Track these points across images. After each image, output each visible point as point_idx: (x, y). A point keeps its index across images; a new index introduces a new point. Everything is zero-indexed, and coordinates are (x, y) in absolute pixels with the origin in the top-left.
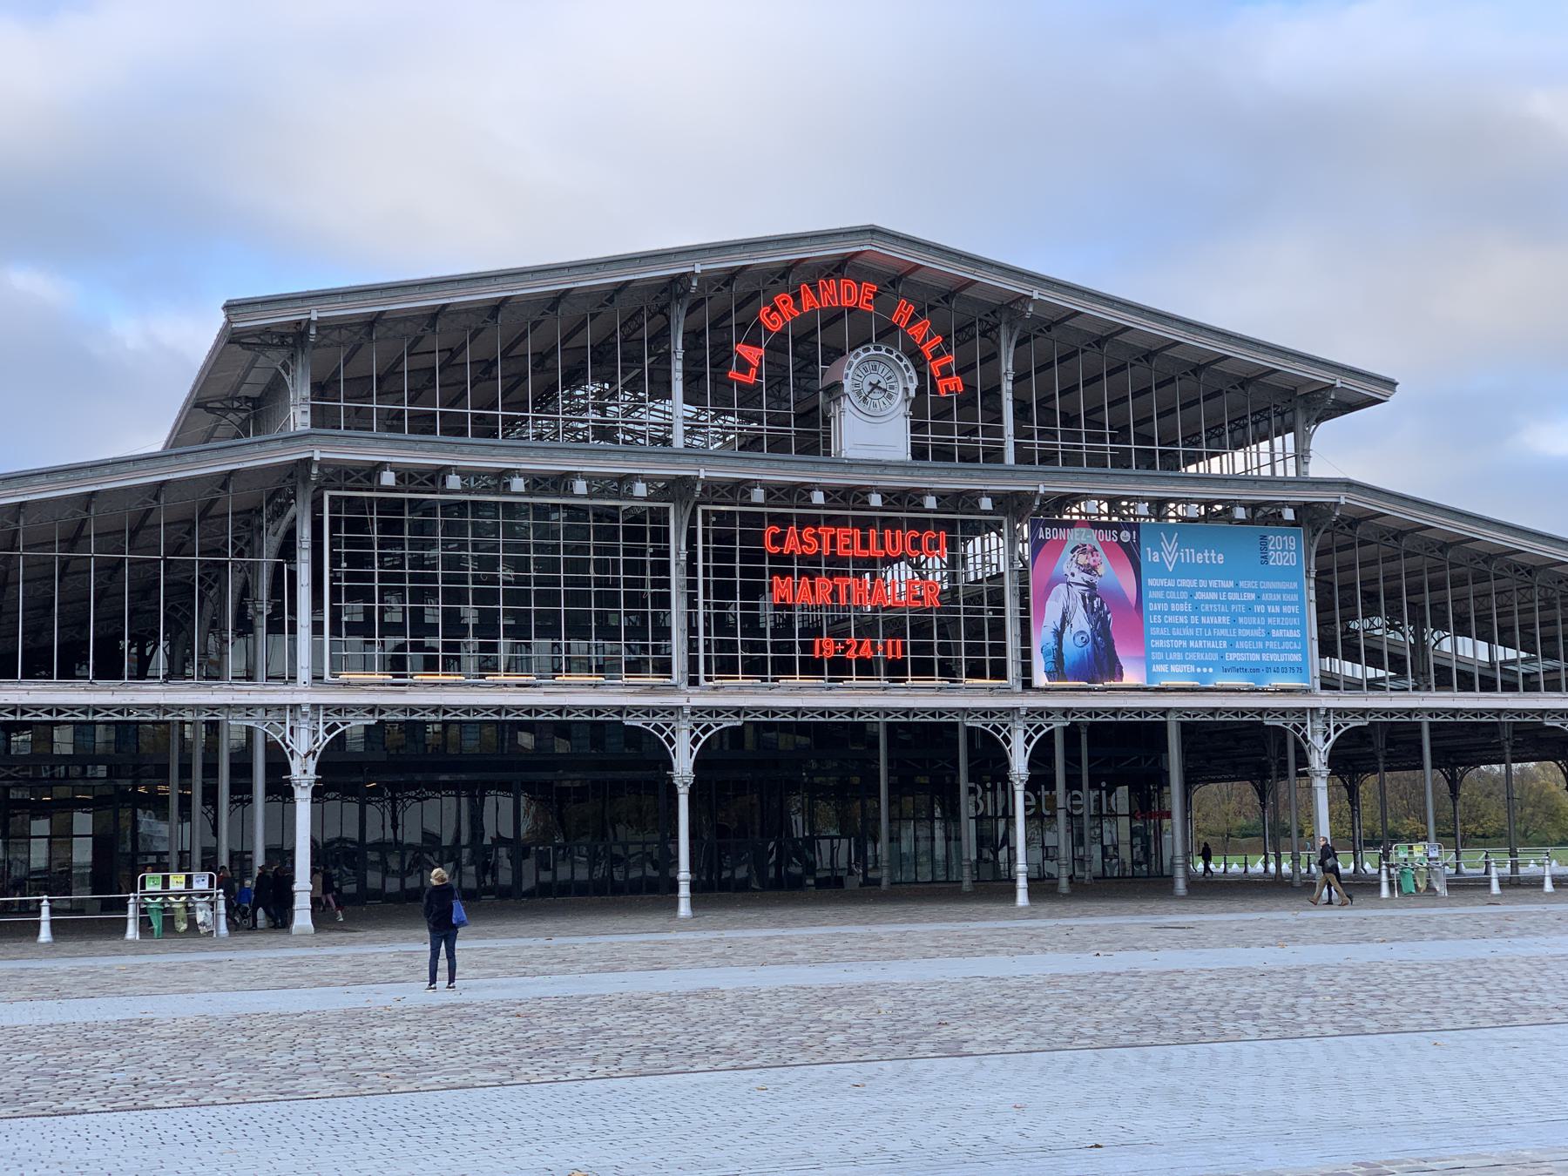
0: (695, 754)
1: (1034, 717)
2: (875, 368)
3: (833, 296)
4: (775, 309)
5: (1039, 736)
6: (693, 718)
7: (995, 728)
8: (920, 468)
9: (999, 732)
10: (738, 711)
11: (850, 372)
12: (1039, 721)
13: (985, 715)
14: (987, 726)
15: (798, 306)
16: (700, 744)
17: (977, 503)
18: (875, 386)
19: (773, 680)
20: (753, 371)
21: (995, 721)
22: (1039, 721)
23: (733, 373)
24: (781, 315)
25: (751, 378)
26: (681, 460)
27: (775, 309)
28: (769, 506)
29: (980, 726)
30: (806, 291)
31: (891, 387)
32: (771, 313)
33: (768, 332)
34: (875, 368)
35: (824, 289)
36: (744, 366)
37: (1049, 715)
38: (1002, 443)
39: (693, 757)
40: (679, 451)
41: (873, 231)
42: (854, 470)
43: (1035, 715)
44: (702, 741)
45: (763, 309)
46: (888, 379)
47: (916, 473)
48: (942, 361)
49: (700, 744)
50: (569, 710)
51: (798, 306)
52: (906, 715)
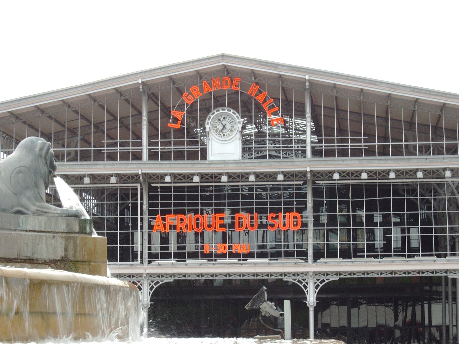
0: (151, 294)
1: (320, 276)
2: (225, 118)
3: (218, 85)
4: (190, 93)
5: (322, 285)
6: (150, 278)
7: (299, 281)
8: (244, 163)
9: (301, 283)
10: (171, 275)
11: (210, 122)
12: (323, 278)
13: (294, 275)
14: (295, 280)
15: (201, 90)
16: (153, 290)
17: (277, 176)
18: (224, 127)
19: (243, 260)
20: (179, 123)
21: (300, 278)
22: (323, 278)
23: (171, 124)
24: (192, 95)
25: (178, 126)
26: (129, 166)
27: (190, 93)
28: (174, 183)
29: (291, 280)
30: (205, 84)
31: (233, 127)
32: (188, 95)
33: (187, 104)
34: (225, 118)
35: (214, 82)
36: (176, 120)
37: (328, 275)
38: (305, 147)
39: (150, 296)
40: (145, 162)
41: (223, 56)
42: (211, 166)
43: (321, 275)
44: (154, 288)
45: (185, 93)
46: (231, 123)
47: (242, 165)
48: (273, 110)
49: (153, 290)
50: (189, 275)
51: (201, 90)
52: (391, 273)
